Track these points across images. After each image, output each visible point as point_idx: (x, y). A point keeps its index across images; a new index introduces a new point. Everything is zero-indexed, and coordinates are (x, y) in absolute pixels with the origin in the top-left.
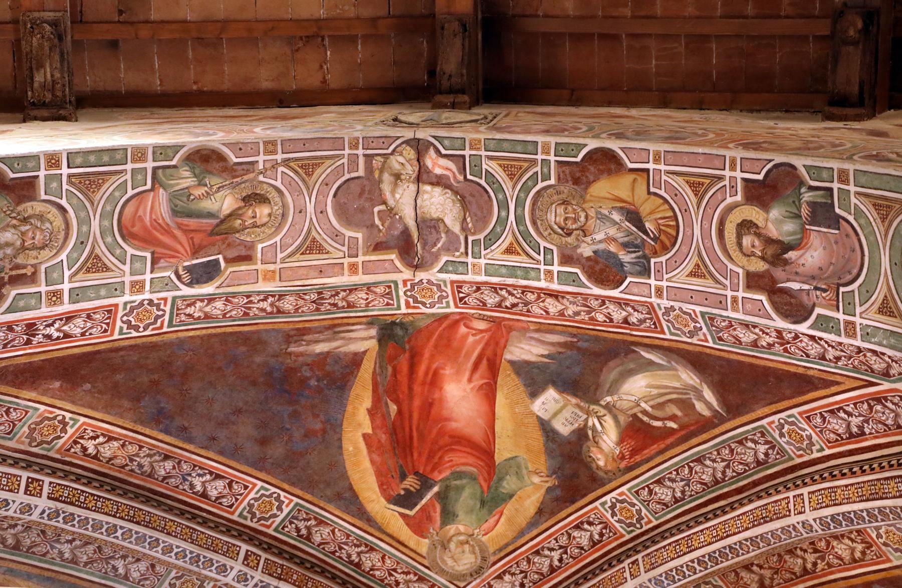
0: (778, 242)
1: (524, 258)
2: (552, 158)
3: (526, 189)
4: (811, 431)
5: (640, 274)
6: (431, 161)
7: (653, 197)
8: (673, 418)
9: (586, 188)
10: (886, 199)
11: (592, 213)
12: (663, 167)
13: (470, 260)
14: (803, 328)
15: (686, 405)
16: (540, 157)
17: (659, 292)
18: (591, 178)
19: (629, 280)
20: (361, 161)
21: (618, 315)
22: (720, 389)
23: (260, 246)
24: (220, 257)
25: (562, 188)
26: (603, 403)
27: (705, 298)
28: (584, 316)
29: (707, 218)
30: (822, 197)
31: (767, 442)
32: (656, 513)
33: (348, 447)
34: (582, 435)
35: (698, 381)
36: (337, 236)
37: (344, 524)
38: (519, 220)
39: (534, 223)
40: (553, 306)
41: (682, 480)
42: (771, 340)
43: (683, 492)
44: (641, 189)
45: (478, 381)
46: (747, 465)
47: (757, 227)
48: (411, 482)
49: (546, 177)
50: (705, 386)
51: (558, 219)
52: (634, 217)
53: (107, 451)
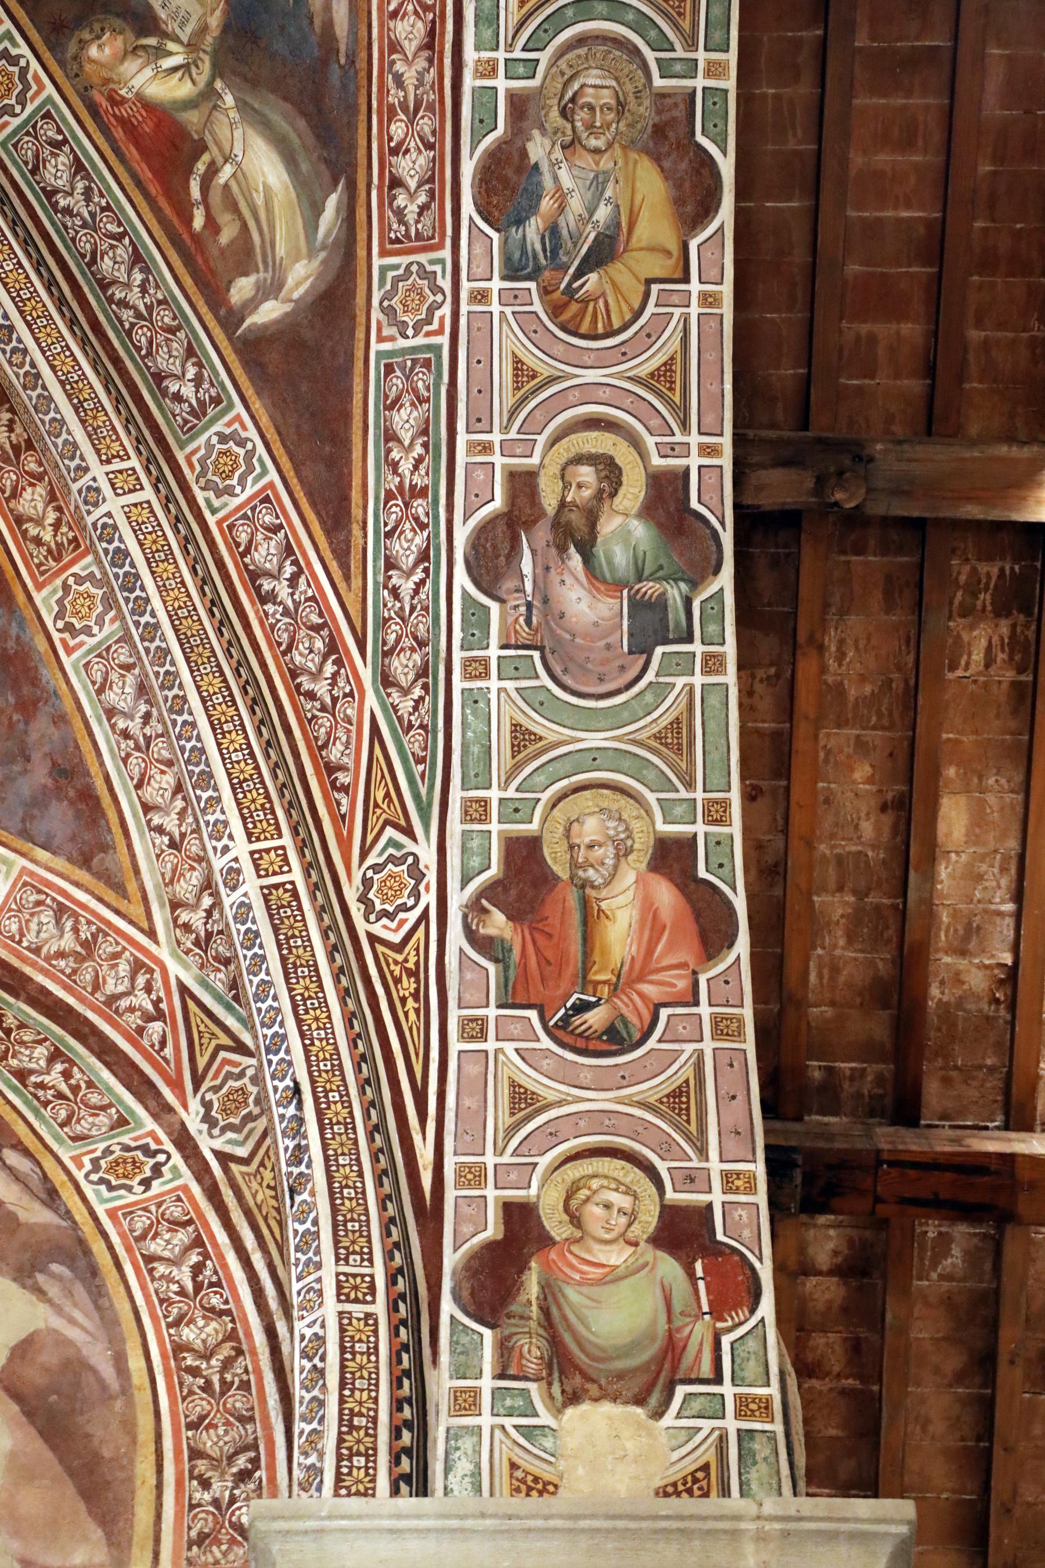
1: (515, 18)
2: (700, 82)
4: (243, 497)
5: (507, 260)
7: (642, 288)
8: (212, 224)
9: (648, 153)
10: (691, 743)
11: (605, 163)
12: (694, 310)
16: (701, 56)
18: (667, 164)
19: (495, 235)
25: (647, 102)
26: (219, 85)
28: (395, 97)
29: (617, 396)
30: (677, 624)
31: (201, 403)
32: (15, 146)
35: (296, 295)
39: (581, 41)
41: (93, 215)
43: (68, 211)
44: (657, 266)
46: (149, 354)
47: (613, 495)
50: (288, 307)
51: (591, 91)
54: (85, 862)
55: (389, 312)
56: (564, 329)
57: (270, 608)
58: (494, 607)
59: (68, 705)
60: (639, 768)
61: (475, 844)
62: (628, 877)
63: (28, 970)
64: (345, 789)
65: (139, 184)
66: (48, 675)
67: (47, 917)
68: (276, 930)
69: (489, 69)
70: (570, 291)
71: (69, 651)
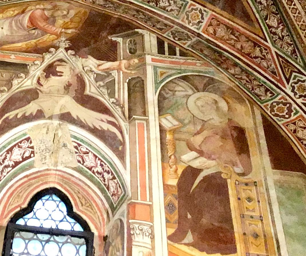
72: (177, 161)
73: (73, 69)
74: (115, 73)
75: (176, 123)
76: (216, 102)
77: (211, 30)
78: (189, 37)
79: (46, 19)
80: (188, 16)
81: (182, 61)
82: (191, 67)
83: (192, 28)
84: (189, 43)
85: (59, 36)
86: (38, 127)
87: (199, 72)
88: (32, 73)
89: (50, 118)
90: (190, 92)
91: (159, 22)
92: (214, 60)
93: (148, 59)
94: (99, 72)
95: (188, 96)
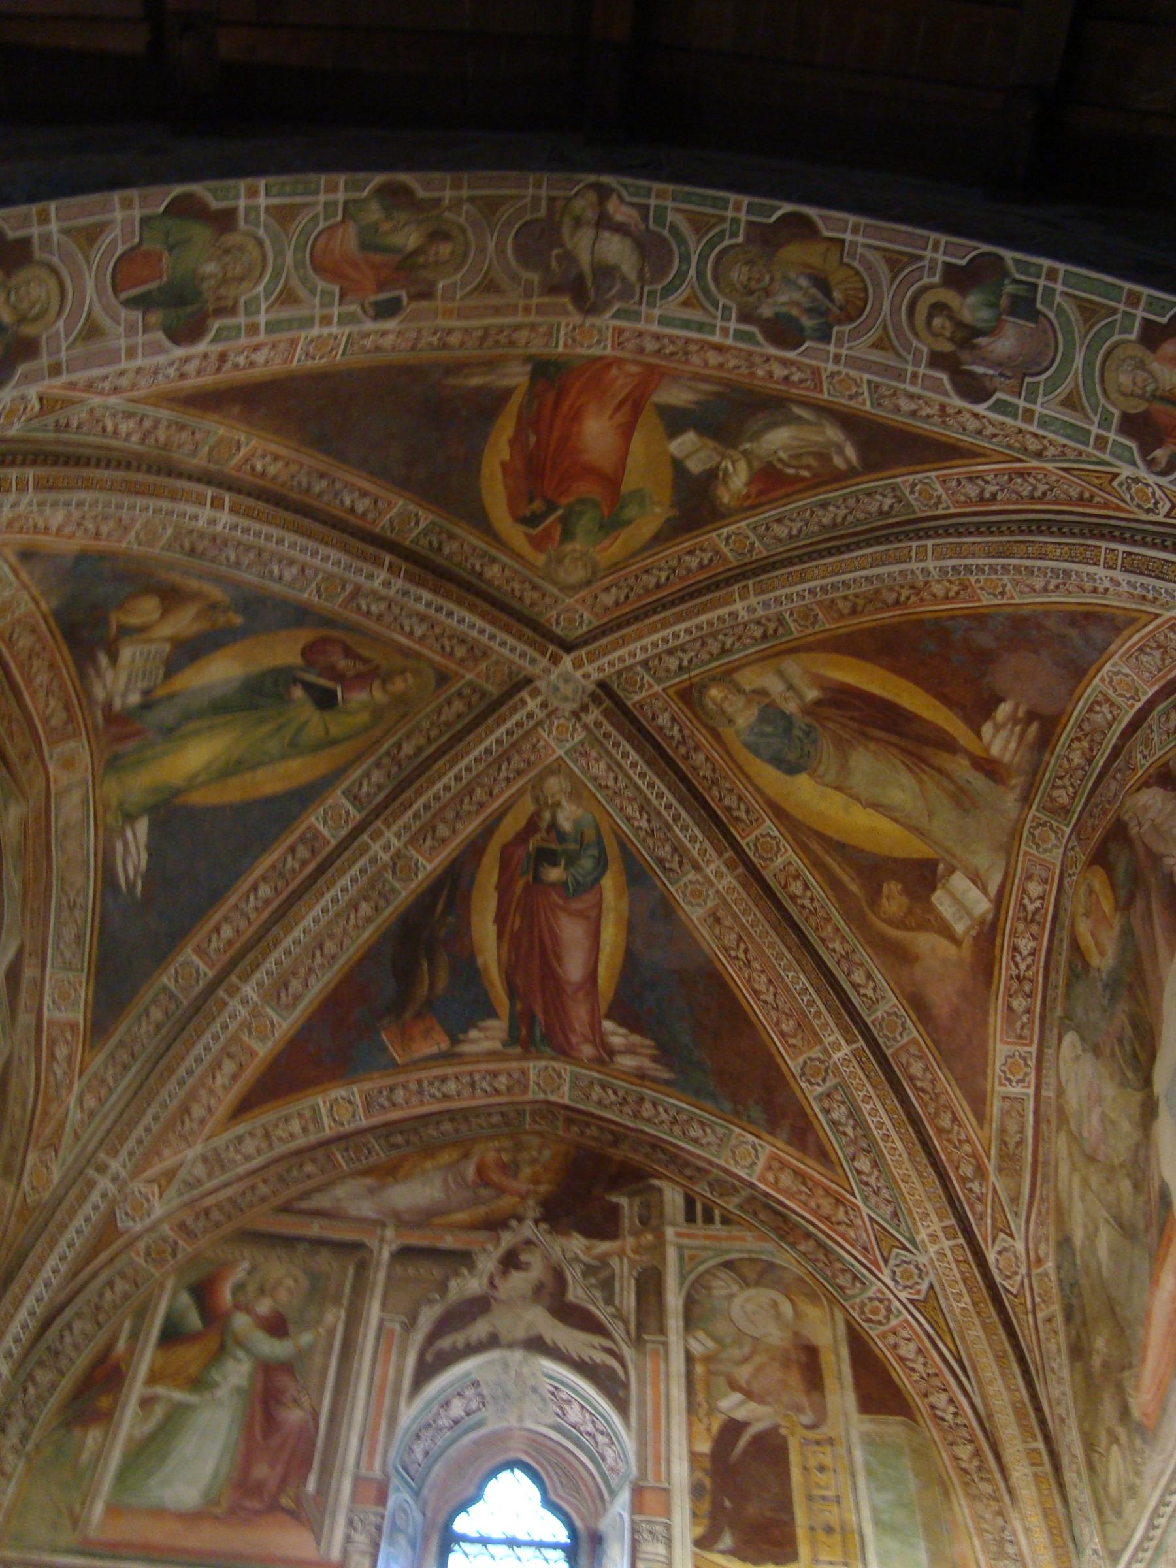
0: (967, 326)
3: (711, 245)
6: (612, 206)
8: (808, 467)
11: (778, 276)
12: (860, 239)
13: (644, 309)
14: (980, 409)
15: (824, 457)
16: (730, 214)
17: (837, 358)
20: (544, 203)
21: (779, 372)
22: (863, 448)
23: (440, 285)
24: (404, 295)
27: (885, 370)
33: (485, 472)
34: (712, 476)
36: (515, 277)
37: (473, 539)
38: (700, 275)
39: (716, 279)
40: (713, 358)
42: (930, 411)
43: (800, 531)
45: (620, 418)
48: (538, 505)
49: (734, 235)
52: (823, 285)
53: (272, 470)
54: (1118, 631)
55: (851, 398)
56: (861, 314)
57: (999, 497)
58: (998, 395)
59: (1040, 608)
60: (1099, 339)
61: (1118, 451)
62: (1156, 366)
63: (1169, 677)
64: (1092, 496)
65: (788, 495)
66: (1024, 611)
67: (1144, 658)
68: (1141, 573)
69: (726, 333)
70: (841, 308)
71: (1012, 598)
72: (712, 1410)
73: (546, 1257)
74: (615, 1262)
75: (711, 1344)
76: (775, 1304)
77: (770, 1177)
78: (735, 1189)
79: (504, 1168)
80: (733, 1153)
81: (724, 1234)
82: (737, 1245)
83: (743, 1174)
84: (736, 1200)
85: (523, 1197)
86: (491, 1363)
87: (750, 1251)
88: (480, 1266)
89: (511, 1346)
90: (735, 1288)
91: (687, 1164)
92: (776, 1230)
93: (670, 1232)
94: (591, 1261)
95: (730, 1297)
